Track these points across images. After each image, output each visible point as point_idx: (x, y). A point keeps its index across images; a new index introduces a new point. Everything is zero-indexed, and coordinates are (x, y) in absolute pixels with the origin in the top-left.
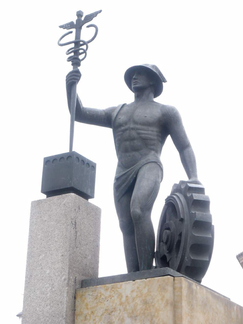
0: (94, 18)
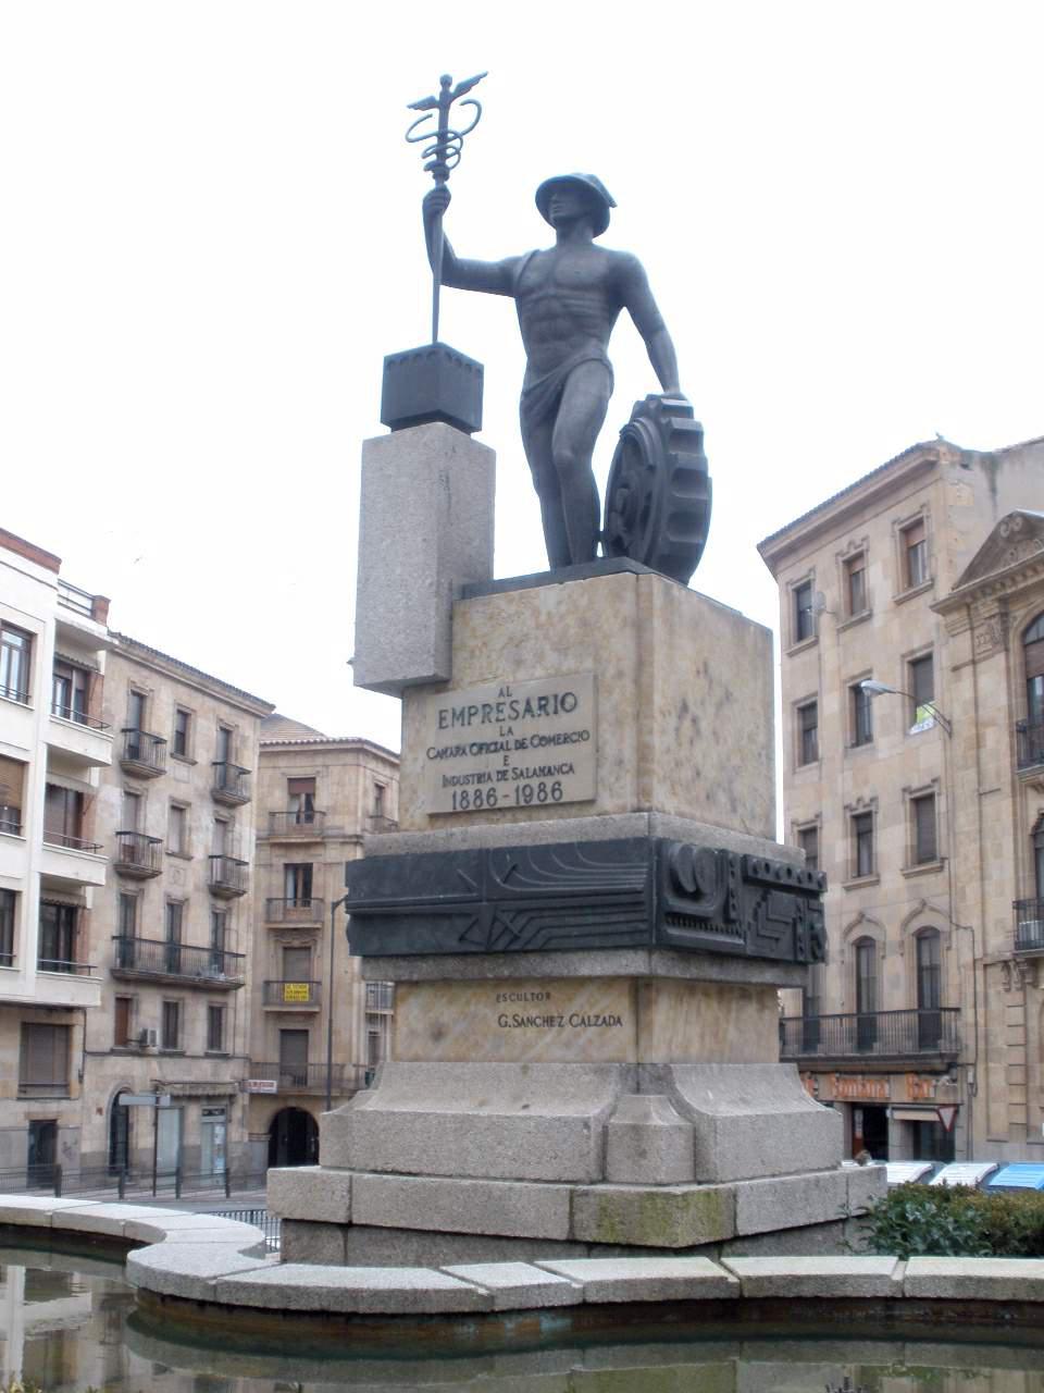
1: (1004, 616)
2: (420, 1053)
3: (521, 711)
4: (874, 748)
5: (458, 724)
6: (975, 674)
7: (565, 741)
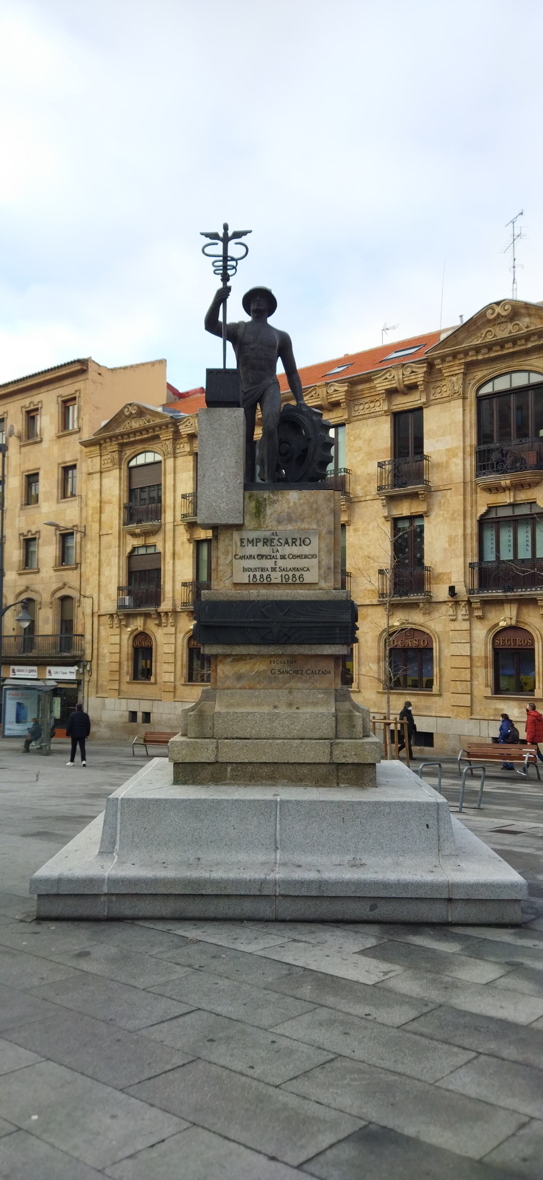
1: (120, 452)
2: (230, 686)
4: (39, 507)
5: (250, 545)
6: (101, 478)
7: (305, 557)
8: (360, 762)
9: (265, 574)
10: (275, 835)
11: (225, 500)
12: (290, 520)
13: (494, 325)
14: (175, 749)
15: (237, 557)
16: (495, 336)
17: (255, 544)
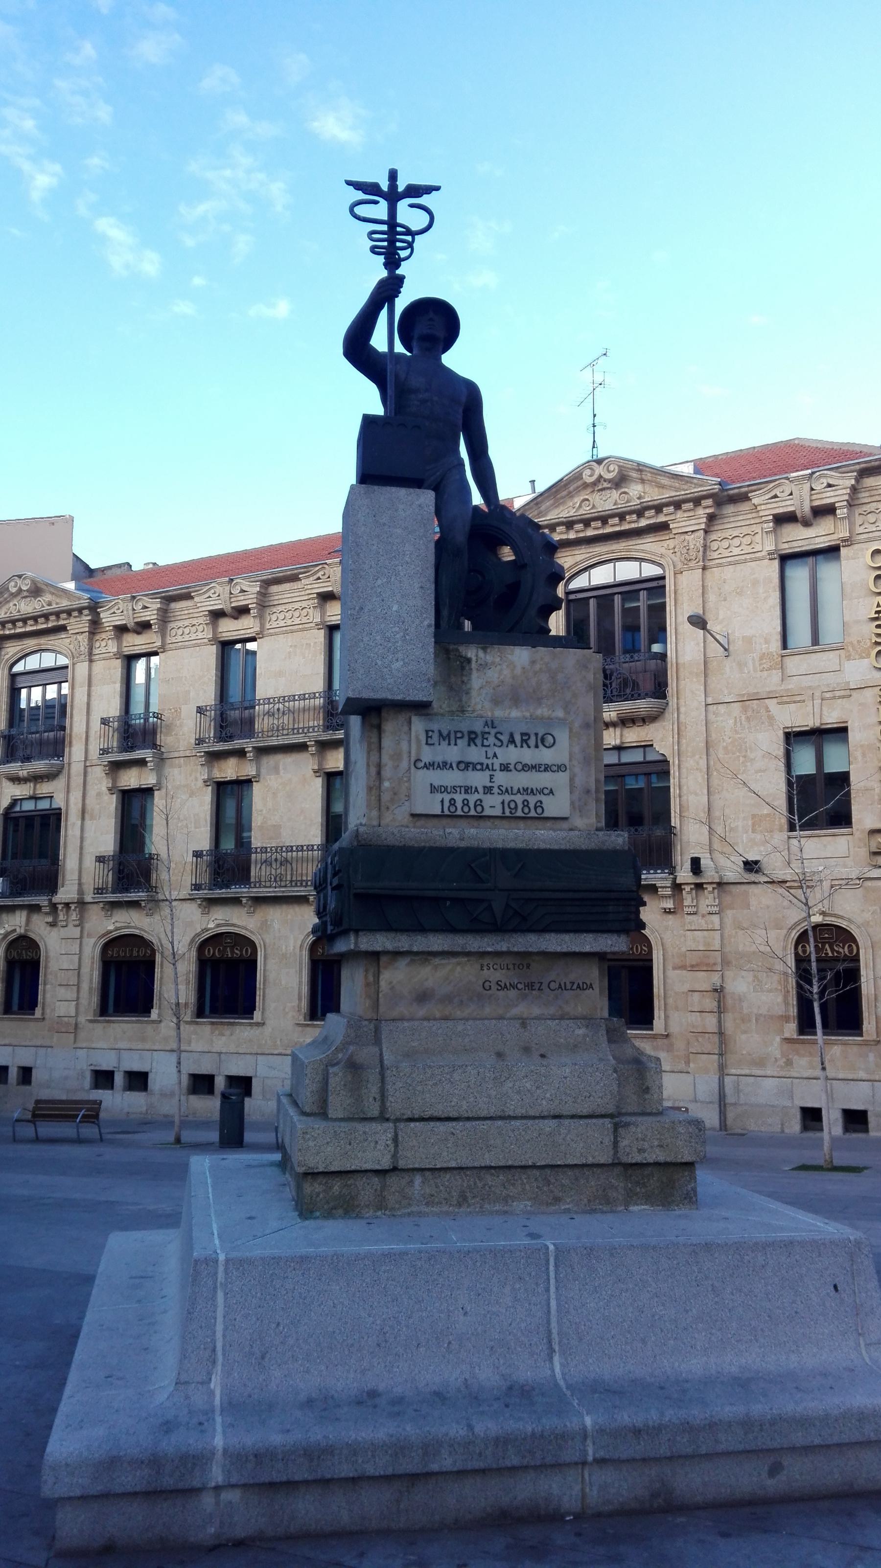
0: (425, 196)
3: (505, 743)
5: (444, 743)
7: (546, 770)
8: (668, 1160)
9: (472, 798)
10: (549, 1322)
11: (400, 655)
12: (516, 700)
13: (593, 491)
14: (311, 1144)
15: (421, 765)
16: (594, 507)
17: (453, 742)
